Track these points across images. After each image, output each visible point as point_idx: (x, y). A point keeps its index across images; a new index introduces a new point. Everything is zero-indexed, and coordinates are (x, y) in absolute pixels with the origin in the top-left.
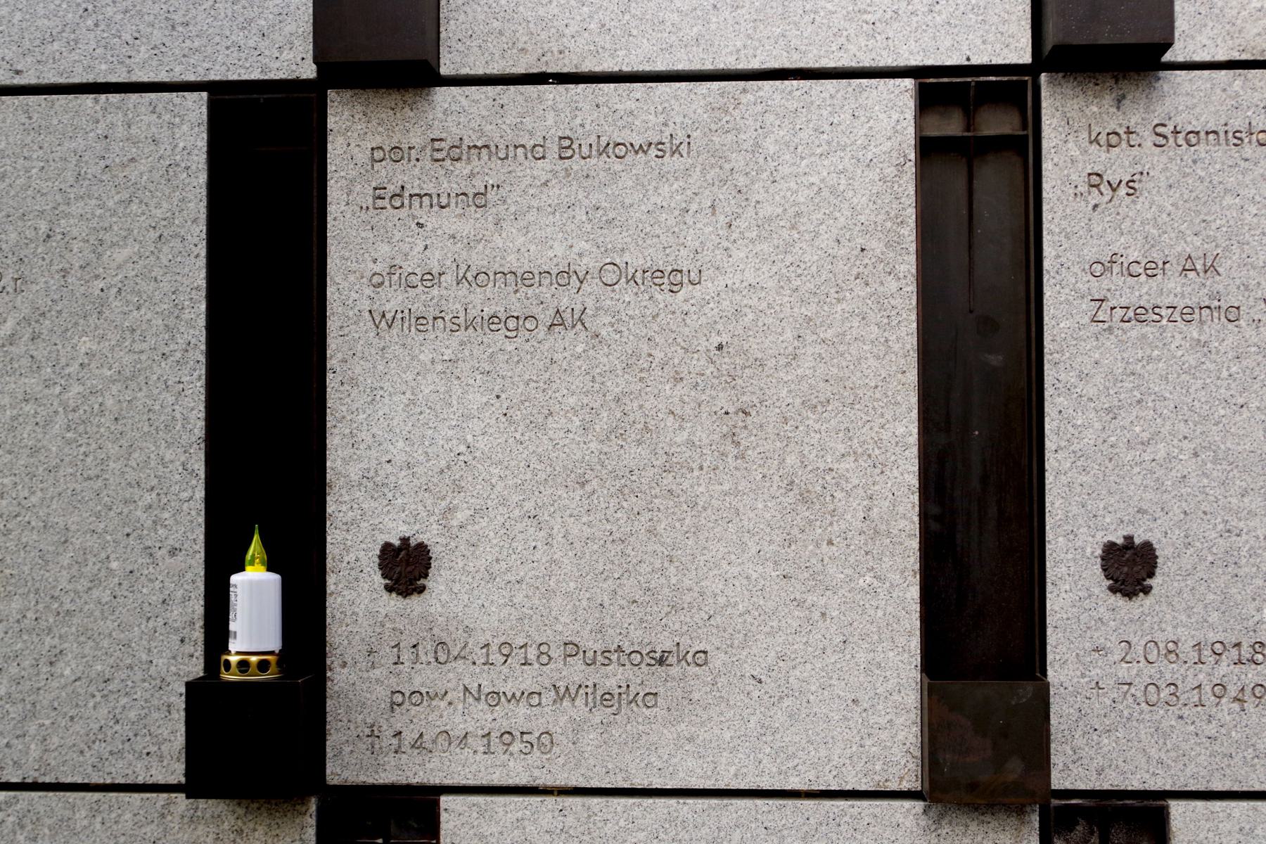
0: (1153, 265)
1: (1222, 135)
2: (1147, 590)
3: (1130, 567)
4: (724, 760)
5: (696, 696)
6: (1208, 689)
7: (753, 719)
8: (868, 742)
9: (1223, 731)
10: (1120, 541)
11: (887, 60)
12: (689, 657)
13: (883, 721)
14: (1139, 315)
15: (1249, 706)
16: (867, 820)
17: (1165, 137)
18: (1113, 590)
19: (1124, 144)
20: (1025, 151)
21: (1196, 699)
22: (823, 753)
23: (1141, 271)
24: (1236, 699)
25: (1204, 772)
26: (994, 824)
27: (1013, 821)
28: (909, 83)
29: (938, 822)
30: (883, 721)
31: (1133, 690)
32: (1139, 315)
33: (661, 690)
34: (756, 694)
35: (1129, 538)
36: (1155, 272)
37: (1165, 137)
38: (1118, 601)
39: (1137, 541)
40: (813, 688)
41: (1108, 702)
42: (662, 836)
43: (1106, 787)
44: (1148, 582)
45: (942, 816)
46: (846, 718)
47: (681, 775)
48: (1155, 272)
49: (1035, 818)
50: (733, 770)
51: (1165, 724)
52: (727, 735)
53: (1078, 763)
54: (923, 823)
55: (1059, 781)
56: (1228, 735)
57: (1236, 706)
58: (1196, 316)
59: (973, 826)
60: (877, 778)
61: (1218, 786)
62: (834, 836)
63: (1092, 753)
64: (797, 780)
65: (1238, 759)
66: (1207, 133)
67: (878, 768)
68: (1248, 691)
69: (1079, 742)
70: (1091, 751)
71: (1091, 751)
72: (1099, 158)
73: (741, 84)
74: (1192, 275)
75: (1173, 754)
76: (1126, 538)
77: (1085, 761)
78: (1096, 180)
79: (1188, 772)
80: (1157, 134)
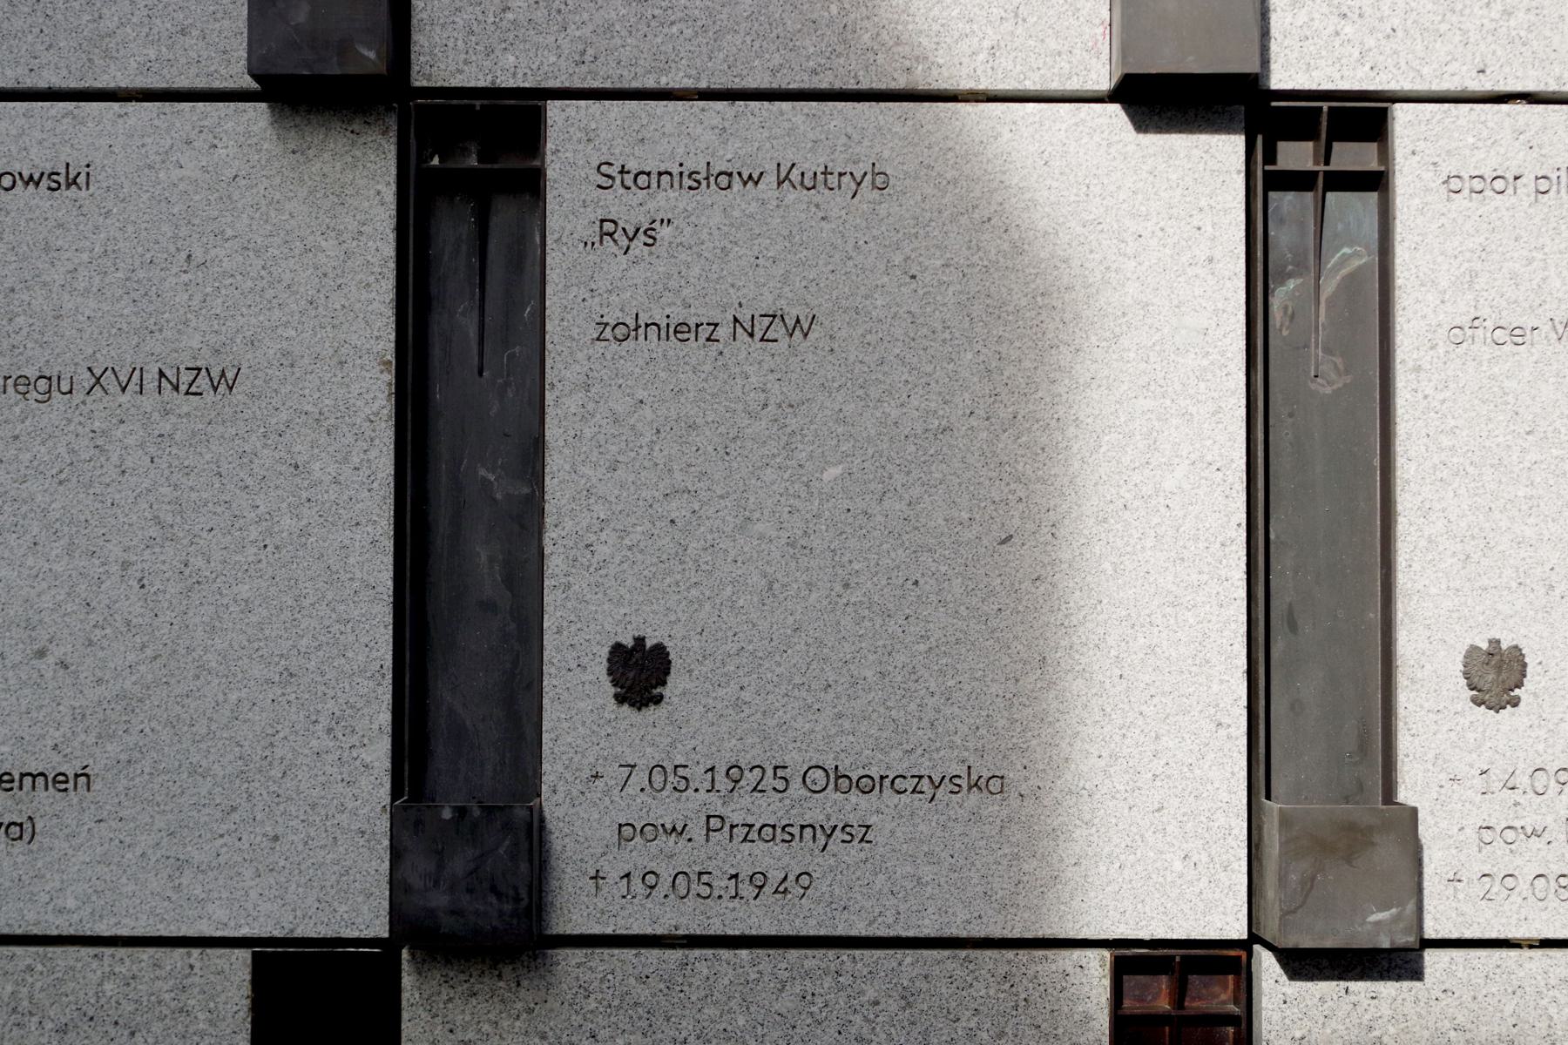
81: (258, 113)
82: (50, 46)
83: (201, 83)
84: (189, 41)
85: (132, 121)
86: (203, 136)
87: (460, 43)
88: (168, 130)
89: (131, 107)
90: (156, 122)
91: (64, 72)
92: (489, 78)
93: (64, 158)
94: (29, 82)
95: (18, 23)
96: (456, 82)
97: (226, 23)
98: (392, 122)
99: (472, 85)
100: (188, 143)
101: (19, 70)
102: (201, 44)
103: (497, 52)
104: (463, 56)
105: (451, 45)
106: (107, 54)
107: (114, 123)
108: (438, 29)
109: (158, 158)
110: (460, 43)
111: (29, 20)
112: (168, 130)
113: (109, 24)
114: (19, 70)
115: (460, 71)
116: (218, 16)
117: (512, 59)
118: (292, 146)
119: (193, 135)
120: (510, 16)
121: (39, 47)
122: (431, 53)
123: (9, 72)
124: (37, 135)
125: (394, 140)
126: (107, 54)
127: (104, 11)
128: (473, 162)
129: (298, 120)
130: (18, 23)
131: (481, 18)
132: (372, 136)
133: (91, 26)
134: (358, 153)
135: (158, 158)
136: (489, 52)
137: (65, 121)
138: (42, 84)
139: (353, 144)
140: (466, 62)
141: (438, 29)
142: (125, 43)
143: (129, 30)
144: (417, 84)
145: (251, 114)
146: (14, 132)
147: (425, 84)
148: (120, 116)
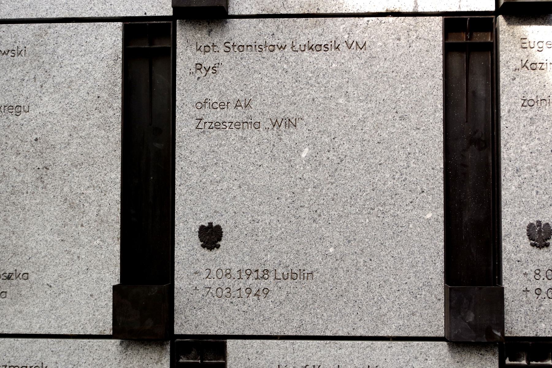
0: (223, 104)
1: (254, 47)
2: (218, 247)
3: (211, 236)
4: (34, 321)
5: (23, 293)
6: (244, 290)
7: (48, 303)
8: (97, 313)
9: (250, 309)
10: (207, 225)
11: (110, 14)
12: (21, 276)
13: (103, 304)
14: (217, 125)
15: (261, 298)
16: (96, 348)
17: (230, 48)
18: (203, 246)
19: (211, 51)
20: (169, 55)
21: (238, 294)
22: (77, 318)
23: (218, 106)
24: (255, 295)
25: (241, 327)
26: (150, 349)
27: (159, 348)
28: (120, 24)
29: (126, 349)
30: (103, 304)
31: (211, 291)
32: (217, 125)
33: (8, 290)
34: (49, 292)
35: (211, 224)
36: (224, 107)
37: (230, 48)
38: (205, 251)
39: (214, 225)
40: (74, 290)
41: (201, 296)
42: (7, 355)
43: (199, 333)
44: (219, 243)
45: (128, 346)
46: (87, 303)
47: (16, 328)
48: (224, 107)
49: (168, 347)
50: (38, 326)
51: (225, 305)
52: (36, 311)
53: (186, 323)
54: (120, 349)
55: (178, 330)
56: (252, 310)
57: (256, 298)
58: (241, 126)
59: (141, 351)
60: (100, 329)
61: (247, 333)
62: (81, 355)
63: (193, 318)
64: (66, 330)
65: (256, 321)
66: (247, 46)
67: (101, 325)
68: (261, 290)
69: (188, 313)
70: (192, 318)
71: (192, 318)
72: (200, 57)
73: (48, 24)
74: (239, 108)
75: (228, 319)
76: (209, 223)
77: (190, 322)
78: (199, 67)
79: (235, 327)
80: (227, 47)
81: (443, 346)
82: (361, 320)
83: (420, 334)
84: (415, 318)
85: (394, 349)
86: (422, 356)
87: (523, 319)
88: (408, 353)
89: (394, 343)
90: (403, 350)
91: (367, 330)
92: (535, 333)
93: (367, 364)
94: (353, 334)
95: (348, 310)
96: (522, 334)
97: (430, 311)
98: (497, 350)
99: (528, 335)
100: (416, 358)
101: (349, 329)
102: (420, 319)
103: (538, 323)
104: (524, 324)
105: (519, 320)
106: (383, 323)
107: (387, 350)
108: (514, 313)
109: (404, 364)
110: (523, 319)
111: (352, 309)
112: (408, 353)
113: (384, 311)
114: (349, 329)
115: (523, 330)
116: (427, 308)
117: (543, 325)
118: (457, 360)
119: (418, 355)
120: (542, 308)
121: (356, 320)
122: (512, 323)
123: (345, 330)
124: (356, 354)
125: (497, 358)
126: (383, 323)
127: (382, 306)
128: (524, 362)
129: (459, 349)
130: (348, 310)
131: (531, 309)
132: (489, 356)
133: (377, 312)
134: (483, 363)
135: (404, 364)
136: (535, 322)
137: (368, 349)
138: (358, 335)
139: (481, 359)
140: (525, 327)
141: (514, 313)
142: (390, 319)
143: (392, 313)
144: (506, 335)
145: (441, 347)
146: (347, 353)
147: (509, 335)
148: (389, 347)
